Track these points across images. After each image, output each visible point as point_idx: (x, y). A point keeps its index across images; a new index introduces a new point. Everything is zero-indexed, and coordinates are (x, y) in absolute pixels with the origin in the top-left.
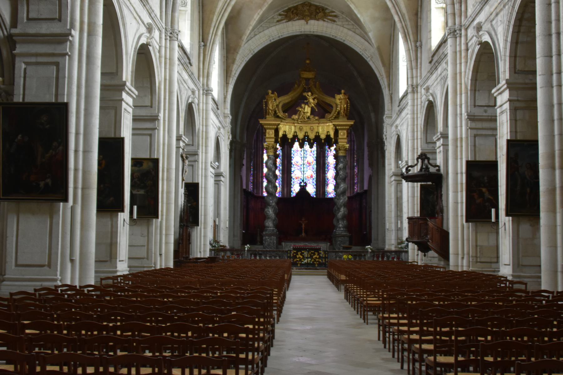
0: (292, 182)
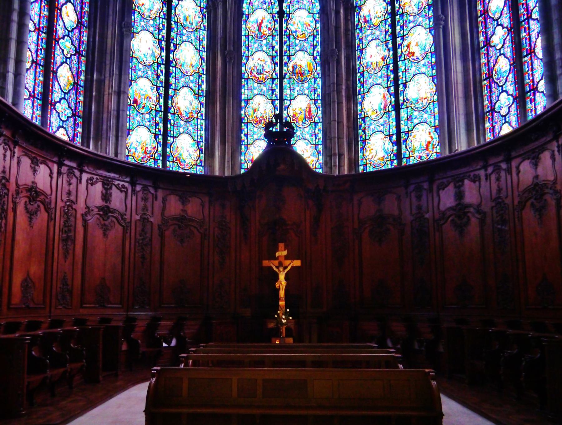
0: (243, 137)
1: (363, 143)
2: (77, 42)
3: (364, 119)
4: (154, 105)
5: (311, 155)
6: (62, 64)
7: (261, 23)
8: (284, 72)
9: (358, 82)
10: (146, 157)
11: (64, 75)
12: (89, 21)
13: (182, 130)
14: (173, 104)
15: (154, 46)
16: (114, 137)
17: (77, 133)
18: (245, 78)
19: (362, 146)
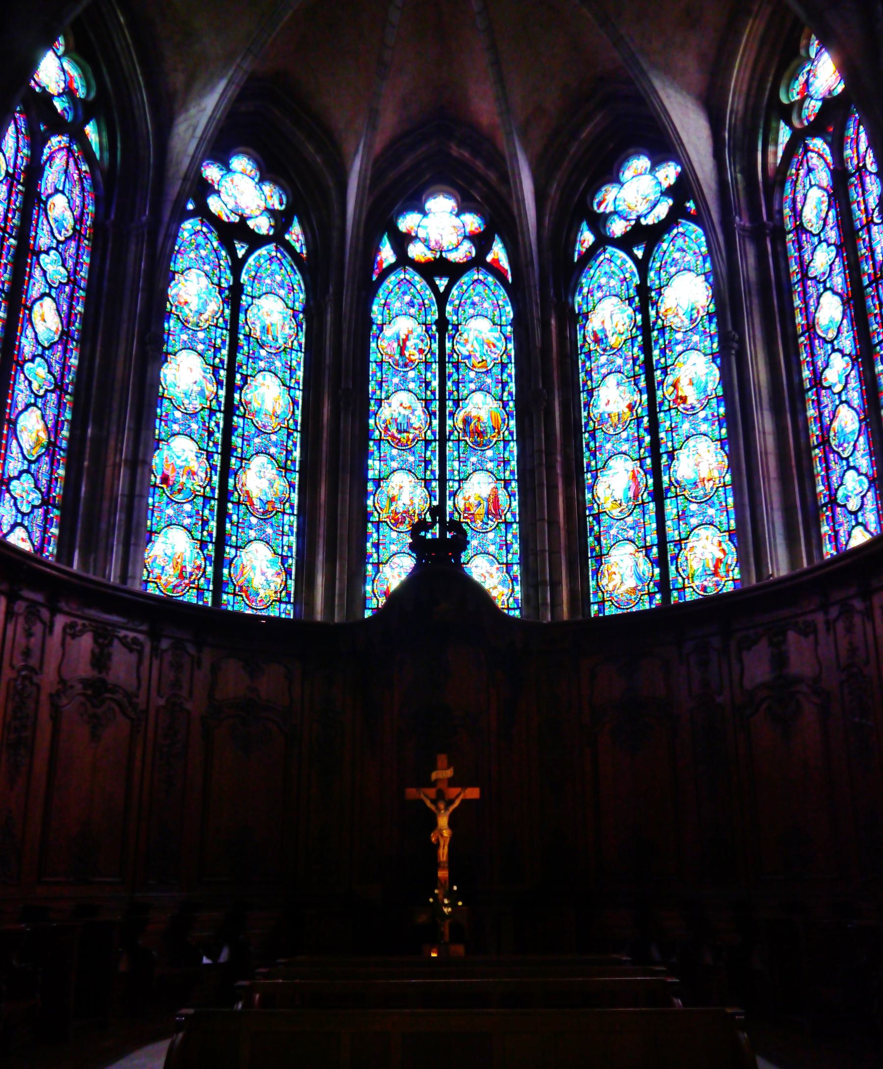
1: (597, 561)
2: (58, 368)
3: (597, 517)
4: (200, 486)
5: (499, 583)
6: (27, 407)
7: (405, 341)
8: (448, 429)
9: (585, 449)
10: (181, 585)
11: (30, 428)
12: (83, 332)
13: (252, 534)
14: (237, 486)
15: (204, 377)
16: (121, 547)
17: (50, 537)
18: (374, 440)
19: (594, 568)
